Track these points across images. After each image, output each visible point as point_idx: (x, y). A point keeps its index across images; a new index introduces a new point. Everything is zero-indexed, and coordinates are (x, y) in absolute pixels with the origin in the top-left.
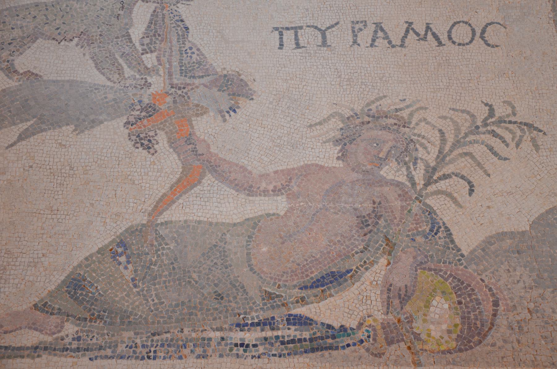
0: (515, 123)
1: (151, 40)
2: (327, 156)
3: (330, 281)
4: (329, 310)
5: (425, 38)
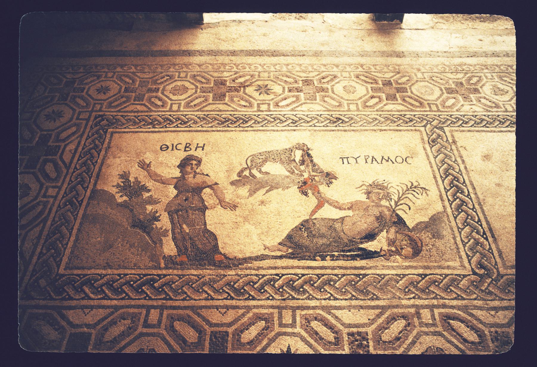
2: (363, 198)
3: (371, 236)
4: (371, 246)
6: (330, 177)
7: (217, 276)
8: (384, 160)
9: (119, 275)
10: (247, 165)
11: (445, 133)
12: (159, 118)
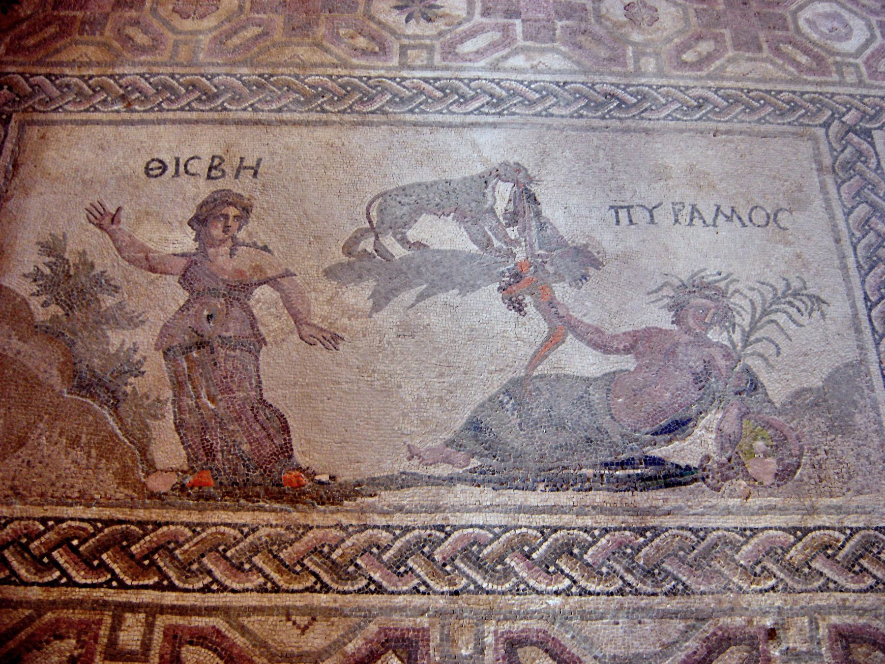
3: (676, 427)
5: (732, 220)
6: (585, 260)
7: (288, 528)
8: (721, 217)
9: (44, 520)
10: (370, 222)
11: (872, 144)
12: (143, 83)
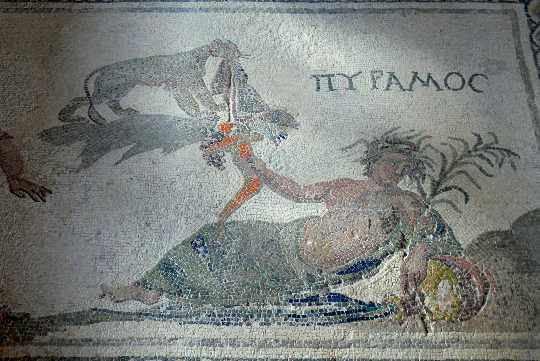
0: (498, 149)
1: (220, 84)
2: (357, 172)
5: (427, 85)
8: (418, 81)
10: (87, 92)
